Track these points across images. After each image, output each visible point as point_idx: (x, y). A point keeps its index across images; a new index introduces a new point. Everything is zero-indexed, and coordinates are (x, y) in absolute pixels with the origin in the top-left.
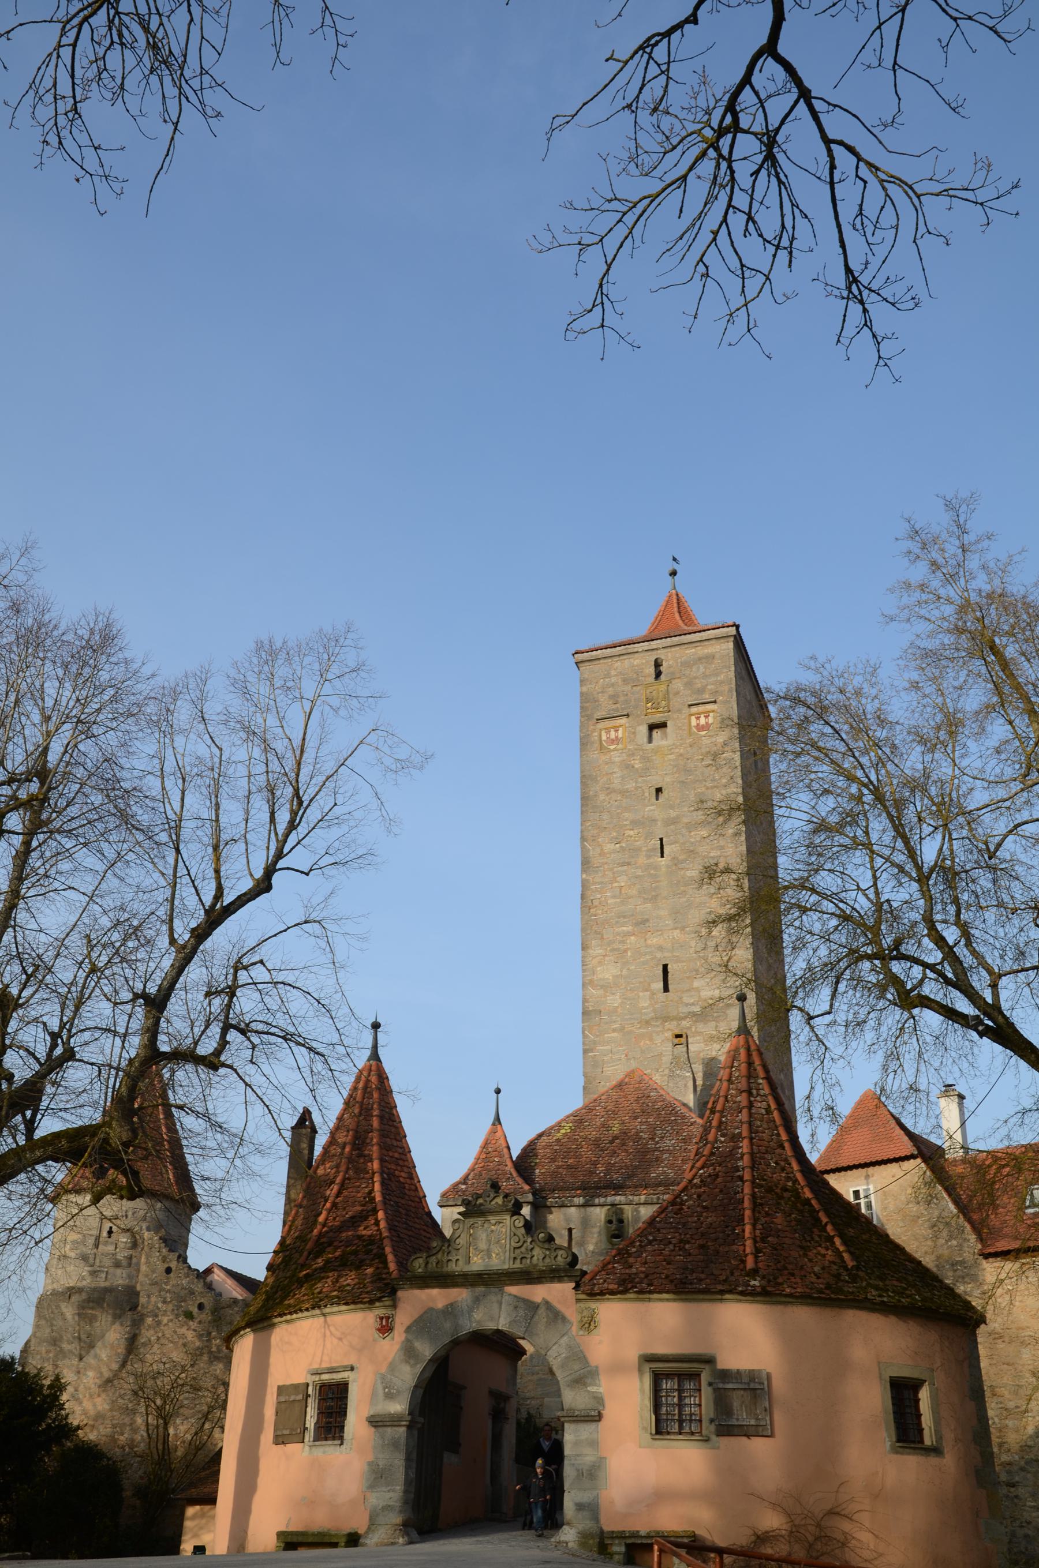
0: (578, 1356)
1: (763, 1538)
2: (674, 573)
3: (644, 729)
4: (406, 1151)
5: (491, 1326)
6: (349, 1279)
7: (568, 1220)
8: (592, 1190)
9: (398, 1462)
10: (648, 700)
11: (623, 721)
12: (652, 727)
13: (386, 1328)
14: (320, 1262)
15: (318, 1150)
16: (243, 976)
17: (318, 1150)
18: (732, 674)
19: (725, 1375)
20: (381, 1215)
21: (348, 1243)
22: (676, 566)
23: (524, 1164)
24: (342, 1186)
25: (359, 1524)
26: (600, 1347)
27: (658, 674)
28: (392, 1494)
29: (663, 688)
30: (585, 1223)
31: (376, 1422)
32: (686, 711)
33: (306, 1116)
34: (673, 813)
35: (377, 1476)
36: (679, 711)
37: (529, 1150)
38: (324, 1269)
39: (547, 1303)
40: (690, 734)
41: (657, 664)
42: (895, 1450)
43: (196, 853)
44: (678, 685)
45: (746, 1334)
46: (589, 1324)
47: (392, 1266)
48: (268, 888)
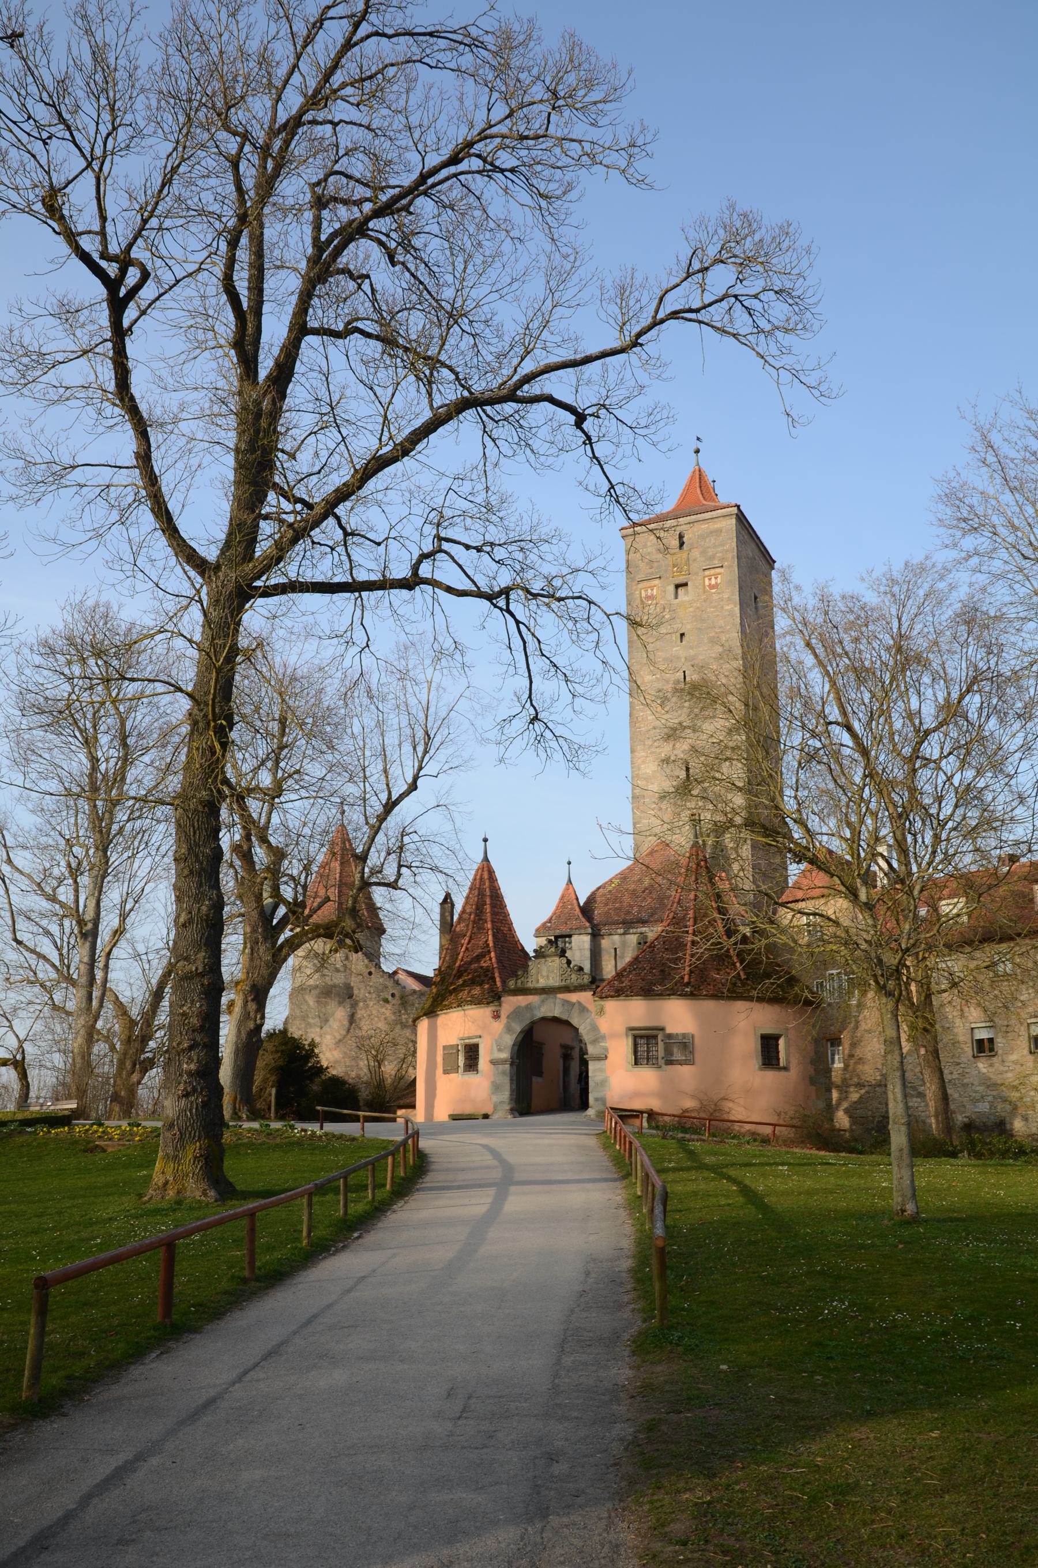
0: (595, 1028)
1: (686, 1111)
2: (697, 451)
3: (671, 588)
4: (506, 915)
5: (550, 1014)
6: (477, 991)
7: (613, 943)
8: (628, 925)
9: (506, 1081)
10: (674, 566)
11: (657, 582)
12: (677, 586)
13: (496, 1016)
14: (461, 981)
15: (456, 917)
16: (406, 839)
17: (456, 917)
18: (734, 544)
19: (670, 1036)
20: (493, 954)
21: (476, 971)
22: (699, 445)
23: (587, 910)
24: (471, 938)
25: (488, 1110)
26: (604, 1025)
27: (682, 544)
28: (505, 1095)
29: (685, 556)
30: (624, 944)
31: (494, 1062)
32: (701, 573)
33: (448, 896)
34: (692, 652)
35: (496, 1088)
36: (697, 574)
37: (591, 899)
38: (463, 985)
39: (579, 1003)
40: (705, 591)
41: (681, 537)
42: (761, 1069)
43: (375, 769)
44: (696, 553)
45: (678, 1015)
46: (601, 1012)
47: (499, 984)
48: (416, 788)
